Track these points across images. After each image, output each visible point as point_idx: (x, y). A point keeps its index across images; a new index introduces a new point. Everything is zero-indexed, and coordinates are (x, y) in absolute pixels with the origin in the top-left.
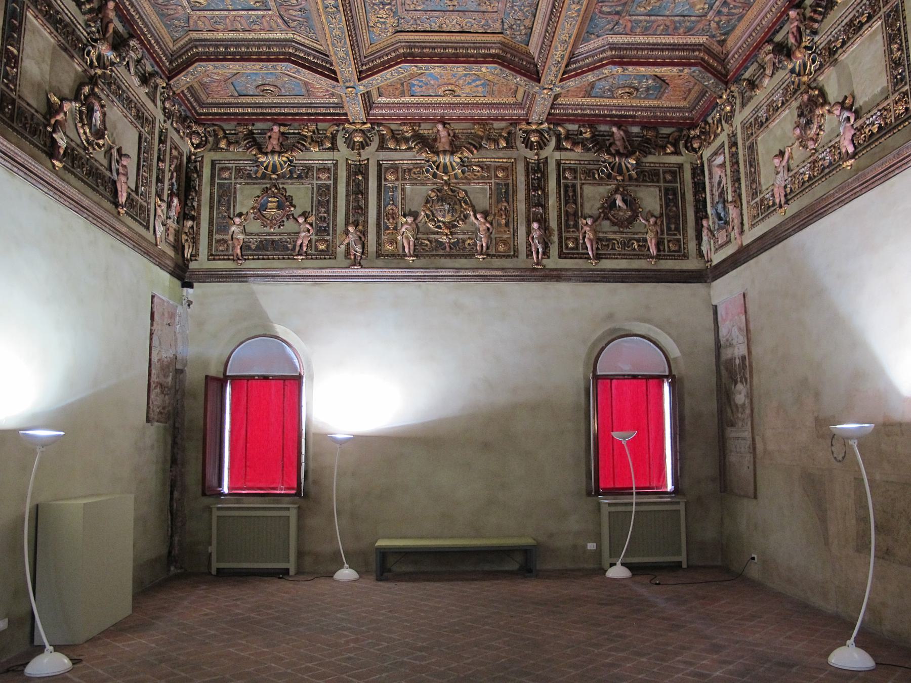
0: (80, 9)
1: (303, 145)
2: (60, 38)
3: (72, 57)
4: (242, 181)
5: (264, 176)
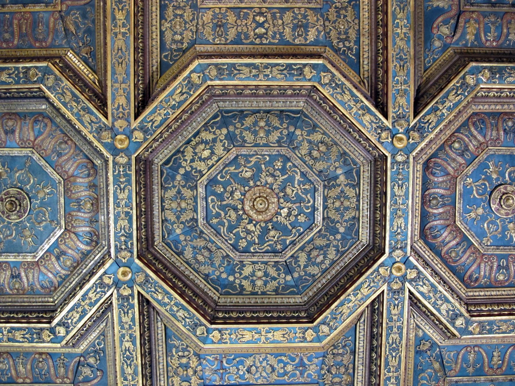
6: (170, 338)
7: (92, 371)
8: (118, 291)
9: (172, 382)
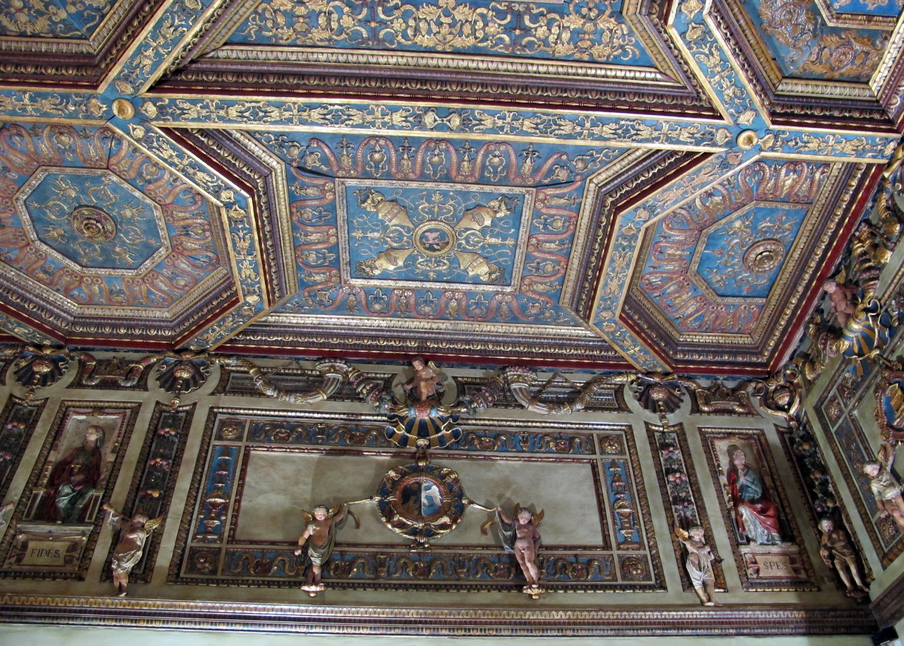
0: (361, 400)
1: (869, 269)
2: (322, 447)
3: (359, 453)
4: (853, 400)
5: (867, 365)
6: (246, 37)
7: (312, 153)
8: (152, 120)
9: (321, 40)
